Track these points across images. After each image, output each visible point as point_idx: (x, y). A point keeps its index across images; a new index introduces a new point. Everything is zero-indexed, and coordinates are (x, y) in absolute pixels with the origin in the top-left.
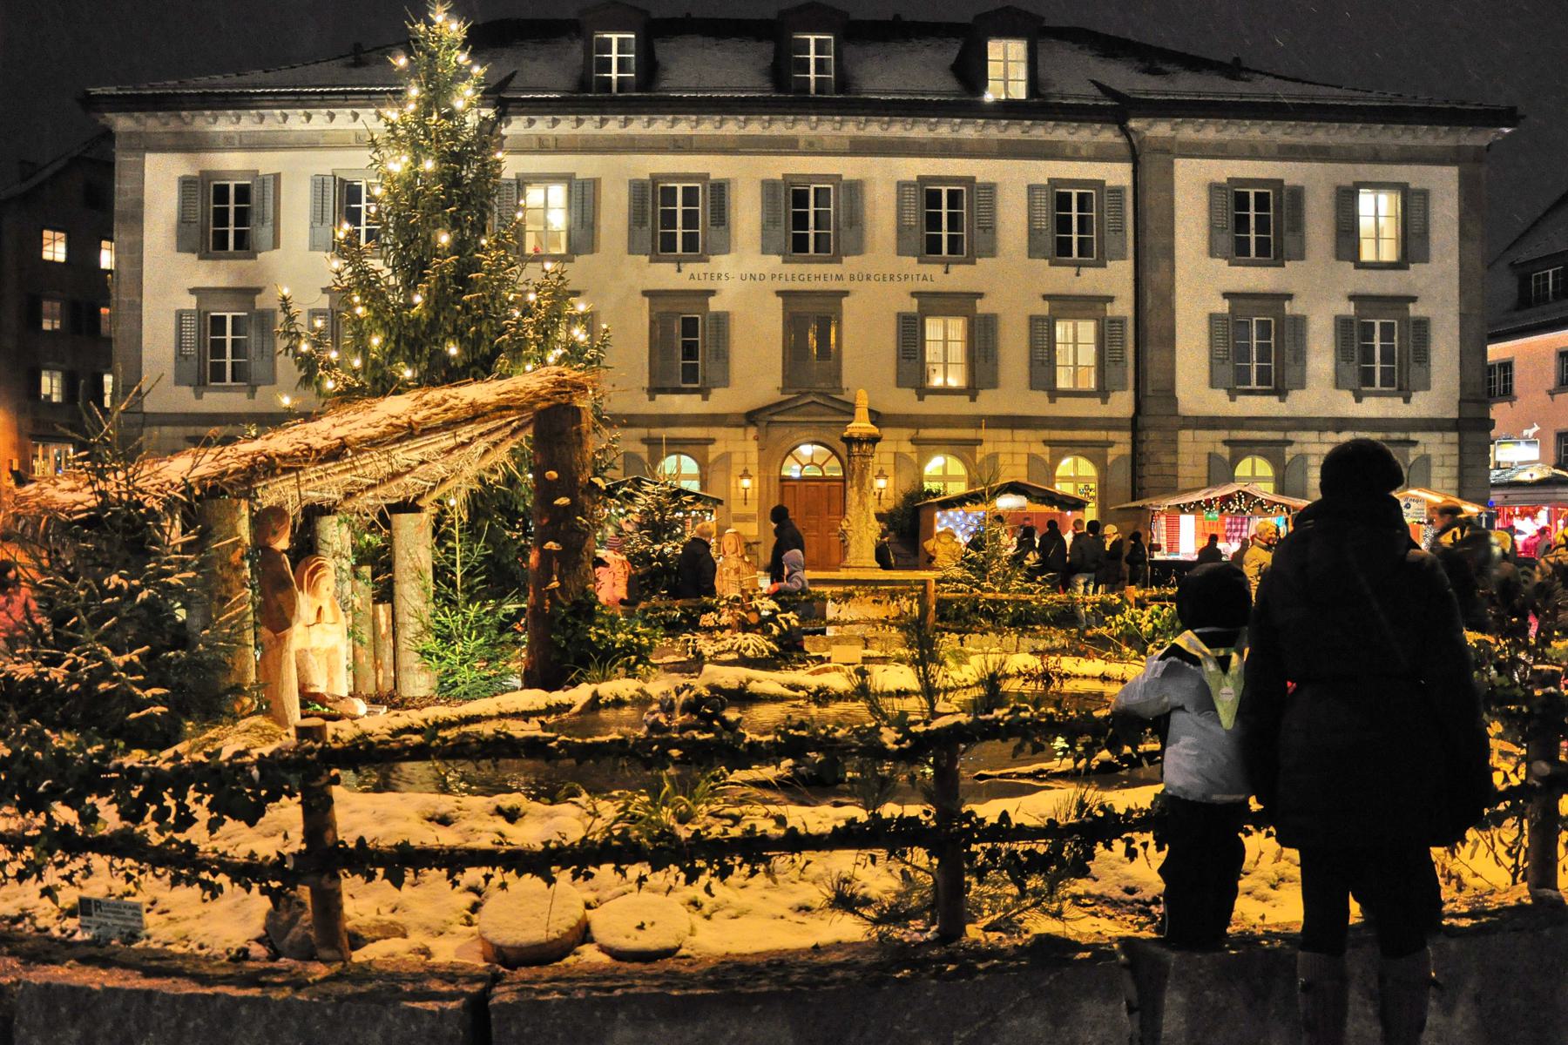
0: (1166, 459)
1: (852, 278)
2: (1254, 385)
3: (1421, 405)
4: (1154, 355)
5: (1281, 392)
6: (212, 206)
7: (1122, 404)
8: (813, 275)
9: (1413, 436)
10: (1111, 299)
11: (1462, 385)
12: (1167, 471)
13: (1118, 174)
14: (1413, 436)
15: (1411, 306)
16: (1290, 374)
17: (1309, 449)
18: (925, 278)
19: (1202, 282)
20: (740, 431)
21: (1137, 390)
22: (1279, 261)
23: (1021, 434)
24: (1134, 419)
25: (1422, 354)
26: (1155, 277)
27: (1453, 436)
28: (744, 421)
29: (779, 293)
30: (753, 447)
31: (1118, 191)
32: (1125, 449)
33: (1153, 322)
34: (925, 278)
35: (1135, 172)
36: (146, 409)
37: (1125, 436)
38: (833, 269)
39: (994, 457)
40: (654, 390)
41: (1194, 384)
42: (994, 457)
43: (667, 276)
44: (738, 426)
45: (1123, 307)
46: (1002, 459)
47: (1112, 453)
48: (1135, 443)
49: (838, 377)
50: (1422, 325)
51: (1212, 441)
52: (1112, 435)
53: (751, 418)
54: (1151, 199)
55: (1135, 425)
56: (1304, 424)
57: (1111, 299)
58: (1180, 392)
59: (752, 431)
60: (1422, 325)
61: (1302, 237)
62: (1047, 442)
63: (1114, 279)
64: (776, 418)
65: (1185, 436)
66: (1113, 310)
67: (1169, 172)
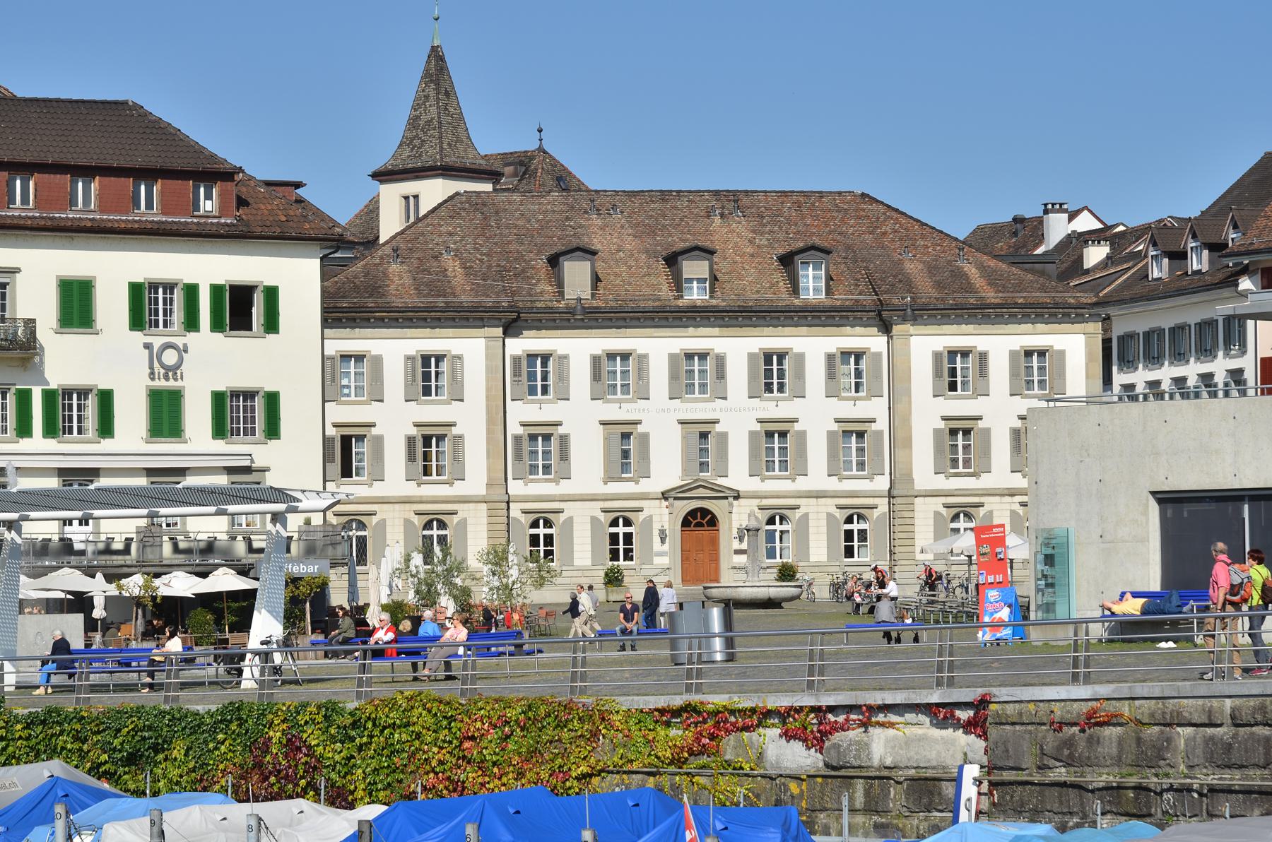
0: (906, 514)
2: (961, 469)
4: (900, 454)
7: (882, 483)
8: (699, 409)
12: (908, 521)
26: (899, 407)
29: (682, 422)
30: (667, 511)
33: (900, 434)
40: (609, 478)
45: (882, 425)
47: (876, 513)
51: (937, 504)
53: (665, 496)
54: (898, 360)
55: (891, 496)
58: (916, 476)
59: (665, 503)
65: (917, 500)
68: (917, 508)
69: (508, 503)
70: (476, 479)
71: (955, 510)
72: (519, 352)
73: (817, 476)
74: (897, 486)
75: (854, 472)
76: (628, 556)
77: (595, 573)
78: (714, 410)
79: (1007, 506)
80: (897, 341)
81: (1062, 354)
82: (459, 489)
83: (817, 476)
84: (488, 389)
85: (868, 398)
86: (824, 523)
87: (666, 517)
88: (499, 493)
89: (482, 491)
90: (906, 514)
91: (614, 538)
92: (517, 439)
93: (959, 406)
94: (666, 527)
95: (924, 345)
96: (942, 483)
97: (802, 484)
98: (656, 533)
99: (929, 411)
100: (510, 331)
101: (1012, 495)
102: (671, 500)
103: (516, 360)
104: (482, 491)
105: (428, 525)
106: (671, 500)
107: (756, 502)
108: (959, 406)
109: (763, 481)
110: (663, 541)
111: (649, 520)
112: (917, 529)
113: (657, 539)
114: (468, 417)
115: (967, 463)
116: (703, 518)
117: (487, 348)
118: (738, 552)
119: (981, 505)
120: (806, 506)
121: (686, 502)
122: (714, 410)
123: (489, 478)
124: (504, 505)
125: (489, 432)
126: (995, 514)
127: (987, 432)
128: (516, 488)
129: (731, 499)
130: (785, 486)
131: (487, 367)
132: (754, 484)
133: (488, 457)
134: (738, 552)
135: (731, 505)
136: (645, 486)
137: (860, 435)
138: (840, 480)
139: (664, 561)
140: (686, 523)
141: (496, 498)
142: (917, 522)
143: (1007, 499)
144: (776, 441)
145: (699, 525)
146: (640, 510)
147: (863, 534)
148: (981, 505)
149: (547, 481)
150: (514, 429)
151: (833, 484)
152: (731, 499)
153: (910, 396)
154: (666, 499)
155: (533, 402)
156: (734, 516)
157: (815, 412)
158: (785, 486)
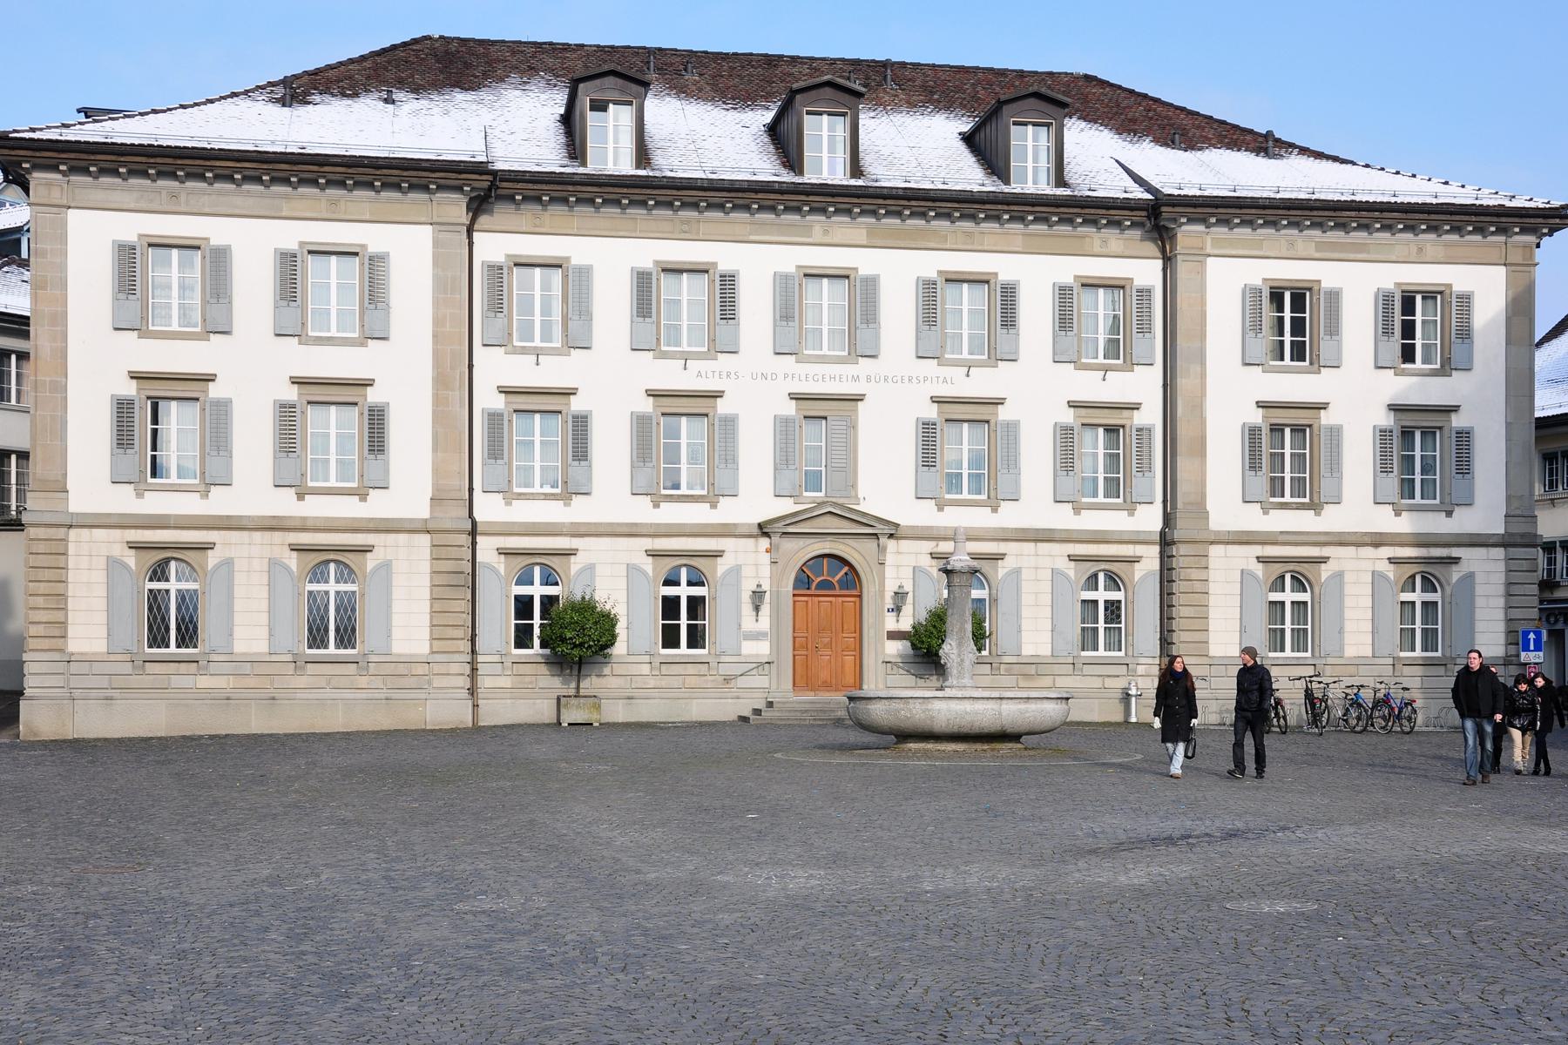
0: (1195, 574)
1: (869, 379)
2: (1287, 498)
3: (1465, 522)
4: (1184, 465)
5: (1315, 507)
6: (1307, 339)
7: (1150, 519)
9: (1455, 552)
10: (1135, 407)
11: (1509, 498)
12: (1198, 586)
13: (1146, 271)
14: (1455, 552)
15: (1453, 416)
16: (1326, 486)
17: (1347, 566)
18: (945, 380)
19: (1235, 389)
20: (752, 540)
21: (1165, 502)
22: (1317, 366)
23: (1044, 547)
24: (1162, 534)
25: (1464, 465)
26: (1184, 383)
27: (1499, 553)
28: (756, 531)
30: (766, 558)
31: (1145, 293)
32: (1155, 565)
33: (1184, 431)
34: (945, 380)
35: (1165, 270)
36: (71, 510)
37: (1157, 548)
38: (848, 370)
39: (1017, 571)
41: (1225, 492)
42: (1017, 571)
43: (673, 376)
44: (750, 536)
45: (1150, 415)
46: (1025, 575)
47: (1139, 571)
48: (1165, 558)
49: (854, 486)
50: (1464, 437)
51: (1245, 556)
52: (1139, 550)
53: (763, 530)
55: (1166, 542)
56: (1342, 540)
57: (1135, 407)
58: (1211, 505)
59: (764, 543)
60: (1464, 437)
61: (1339, 343)
62: (1071, 558)
63: (1141, 387)
64: (790, 530)
65: (1215, 551)
66: (1139, 419)
67: (1202, 273)
68: (1213, 563)
69: (473, 533)
70: (409, 485)
71: (1278, 569)
72: (499, 258)
73: (1035, 500)
74: (1180, 523)
75: (1101, 499)
76: (696, 639)
77: (634, 670)
78: (856, 379)
79: (1368, 566)
80: (1183, 268)
81: (1466, 300)
82: (378, 506)
83: (1035, 500)
84: (438, 322)
85: (1129, 365)
86: (1047, 587)
87: (766, 571)
88: (455, 516)
89: (420, 509)
90: (1195, 574)
91: (670, 607)
92: (494, 419)
93: (1293, 385)
94: (766, 587)
95: (1229, 276)
96: (1254, 519)
97: (1010, 516)
98: (746, 596)
99: (1235, 389)
100: (483, 220)
101: (1376, 545)
102: (776, 539)
103: (495, 271)
104: (420, 509)
105: (318, 574)
106: (776, 539)
107: (929, 546)
108: (1293, 385)
109: (940, 509)
110: (757, 609)
111: (736, 570)
112: (1212, 601)
113: (747, 609)
114: (402, 374)
115: (1299, 487)
116: (833, 573)
117: (436, 243)
118: (893, 635)
119: (1323, 560)
120: (1018, 555)
121: (801, 542)
122: (856, 379)
123: (436, 487)
124: (465, 540)
125: (438, 401)
126: (1348, 578)
127: (1335, 432)
128: (488, 509)
129: (883, 540)
130: (980, 518)
131: (436, 278)
132: (921, 515)
133: (435, 449)
134: (893, 635)
135: (882, 550)
136: (728, 512)
137: (1112, 430)
138: (1077, 510)
139: (762, 649)
140: (803, 581)
141: (448, 525)
142: (1212, 588)
143: (1368, 551)
144: (963, 438)
145: (826, 585)
146: (717, 554)
147: (1113, 609)
148: (1323, 560)
149: (547, 497)
150: (488, 399)
151: (1063, 518)
152: (883, 540)
153: (1203, 363)
154: (766, 535)
155: (524, 351)
156: (889, 572)
157: (1038, 390)
158: (980, 518)
